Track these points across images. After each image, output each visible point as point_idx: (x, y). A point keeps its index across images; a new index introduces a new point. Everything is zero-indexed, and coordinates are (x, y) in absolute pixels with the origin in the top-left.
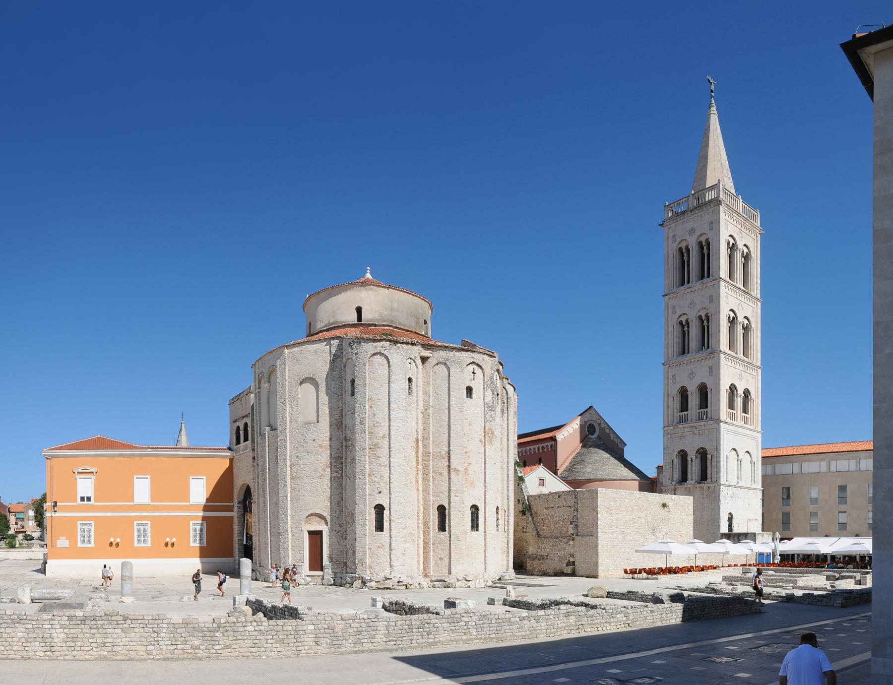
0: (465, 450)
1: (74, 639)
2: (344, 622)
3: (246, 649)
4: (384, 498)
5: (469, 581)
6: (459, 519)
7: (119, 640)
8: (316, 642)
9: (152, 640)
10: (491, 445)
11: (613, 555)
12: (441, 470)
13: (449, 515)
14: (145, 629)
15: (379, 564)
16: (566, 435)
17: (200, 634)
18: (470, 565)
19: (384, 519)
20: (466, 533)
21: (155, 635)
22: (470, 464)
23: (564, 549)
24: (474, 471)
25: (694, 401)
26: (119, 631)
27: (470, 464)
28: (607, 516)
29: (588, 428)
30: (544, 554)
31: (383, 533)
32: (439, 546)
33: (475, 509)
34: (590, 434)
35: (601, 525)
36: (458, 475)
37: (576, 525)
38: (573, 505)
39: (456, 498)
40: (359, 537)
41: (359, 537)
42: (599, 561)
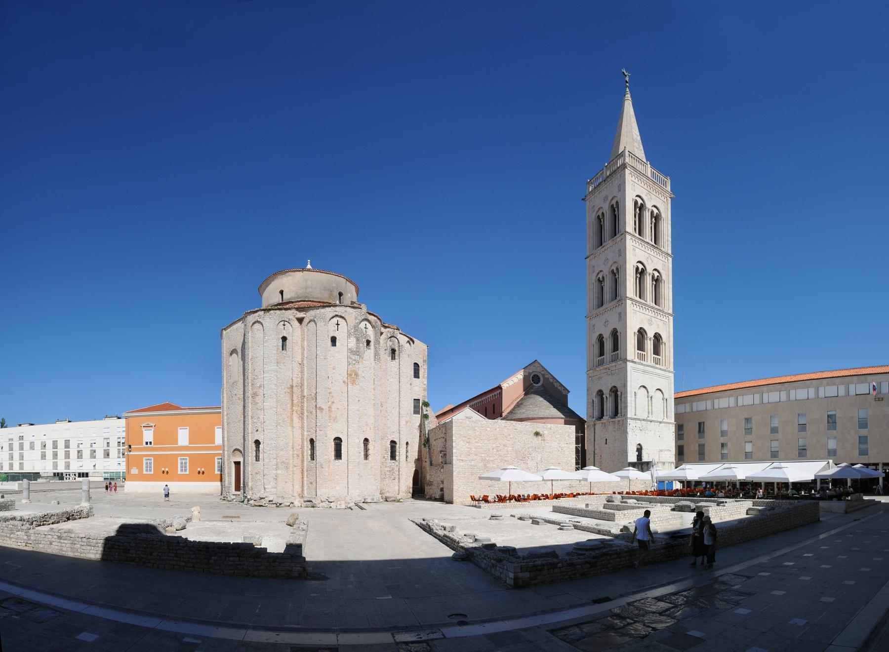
0: (329, 391)
5: (331, 502)
6: (326, 449)
10: (355, 385)
11: (472, 482)
18: (333, 488)
20: (330, 462)
22: (333, 402)
24: (338, 409)
25: (608, 345)
27: (333, 402)
28: (464, 445)
29: (533, 378)
33: (338, 442)
35: (456, 453)
36: (322, 412)
39: (321, 432)
42: (454, 487)
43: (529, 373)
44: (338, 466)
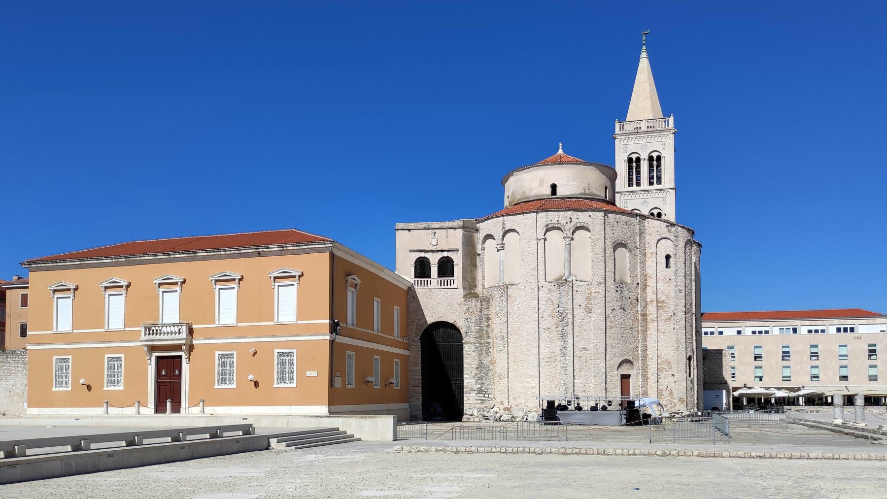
40: (680, 381)
41: (680, 381)
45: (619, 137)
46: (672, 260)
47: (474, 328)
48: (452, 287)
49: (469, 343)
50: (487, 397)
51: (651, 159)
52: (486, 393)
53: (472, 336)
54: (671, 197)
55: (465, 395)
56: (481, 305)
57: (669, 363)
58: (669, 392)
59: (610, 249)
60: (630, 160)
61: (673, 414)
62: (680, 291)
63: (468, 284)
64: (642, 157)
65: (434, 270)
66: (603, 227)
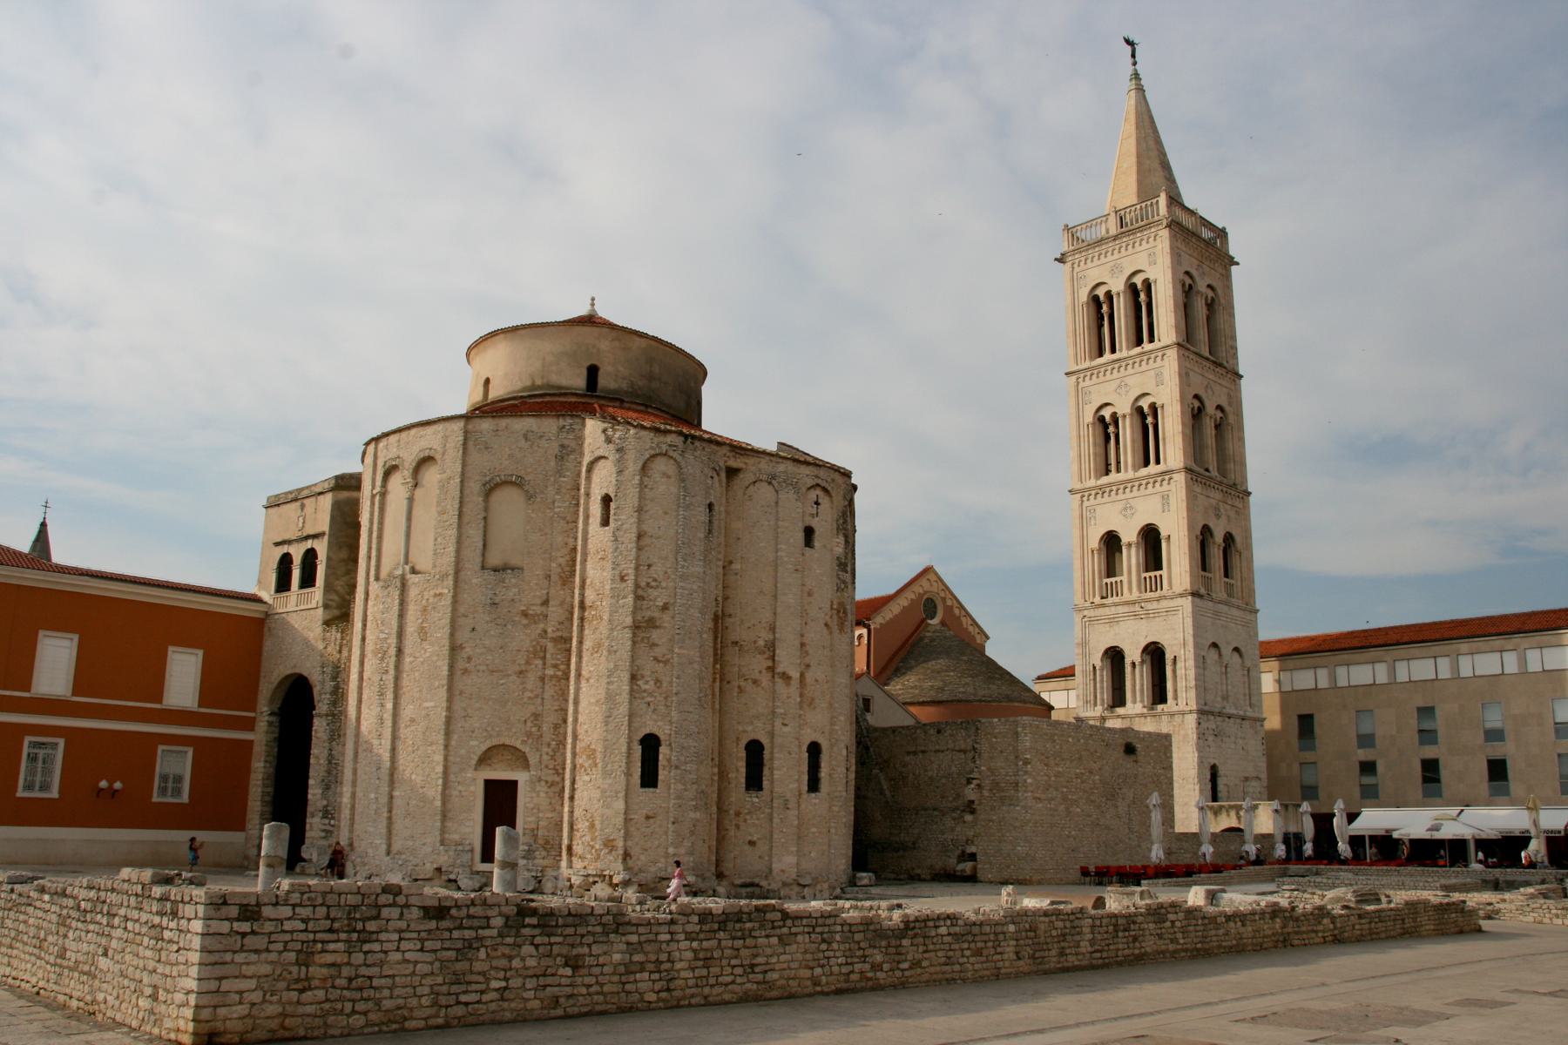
1: (708, 961)
2: (1047, 919)
3: (938, 968)
4: (659, 723)
7: (774, 960)
8: (1017, 953)
9: (821, 955)
12: (756, 675)
13: (772, 759)
14: (813, 936)
15: (646, 850)
16: (887, 619)
17: (884, 943)
19: (660, 763)
21: (824, 947)
23: (953, 830)
24: (816, 681)
26: (774, 940)
27: (808, 666)
29: (924, 604)
30: (907, 839)
31: (658, 791)
32: (748, 817)
33: (814, 750)
34: (927, 617)
36: (788, 684)
37: (978, 785)
38: (969, 748)
39: (786, 729)
43: (919, 594)
44: (815, 804)
45: (1070, 258)
46: (613, 505)
47: (330, 685)
48: (310, 606)
49: (320, 716)
50: (333, 826)
51: (1133, 290)
52: (333, 818)
53: (326, 701)
54: (1170, 364)
55: (308, 821)
56: (342, 639)
57: (591, 754)
58: (587, 824)
59: (475, 500)
60: (1095, 300)
61: (591, 880)
62: (622, 579)
63: (336, 598)
64: (1114, 292)
65: (296, 574)
66: (461, 451)
